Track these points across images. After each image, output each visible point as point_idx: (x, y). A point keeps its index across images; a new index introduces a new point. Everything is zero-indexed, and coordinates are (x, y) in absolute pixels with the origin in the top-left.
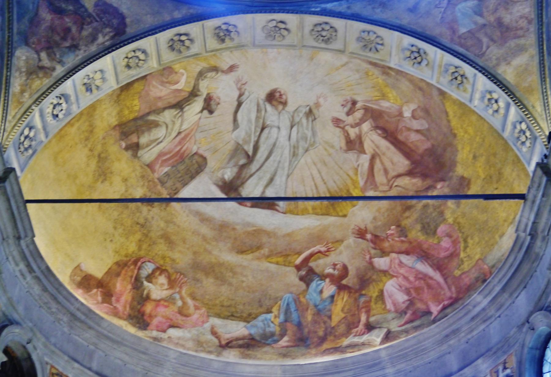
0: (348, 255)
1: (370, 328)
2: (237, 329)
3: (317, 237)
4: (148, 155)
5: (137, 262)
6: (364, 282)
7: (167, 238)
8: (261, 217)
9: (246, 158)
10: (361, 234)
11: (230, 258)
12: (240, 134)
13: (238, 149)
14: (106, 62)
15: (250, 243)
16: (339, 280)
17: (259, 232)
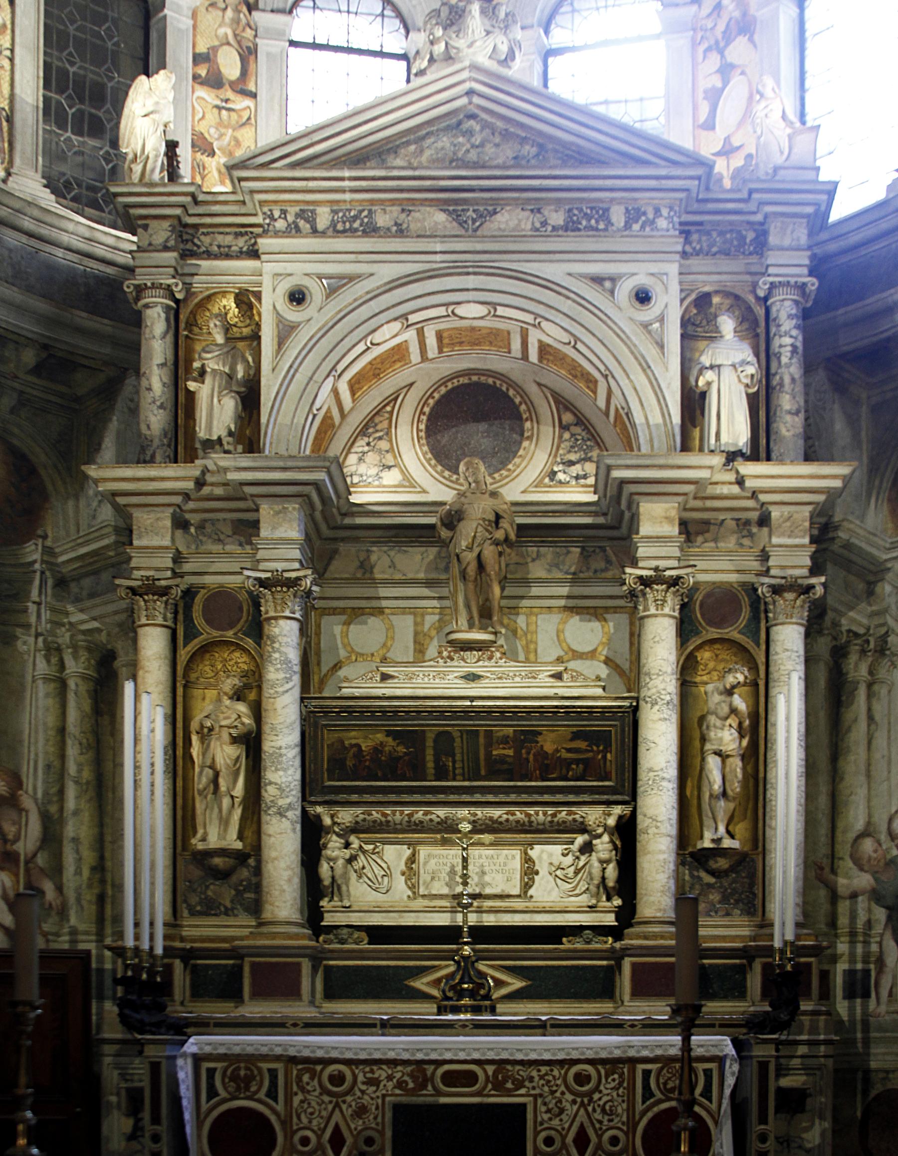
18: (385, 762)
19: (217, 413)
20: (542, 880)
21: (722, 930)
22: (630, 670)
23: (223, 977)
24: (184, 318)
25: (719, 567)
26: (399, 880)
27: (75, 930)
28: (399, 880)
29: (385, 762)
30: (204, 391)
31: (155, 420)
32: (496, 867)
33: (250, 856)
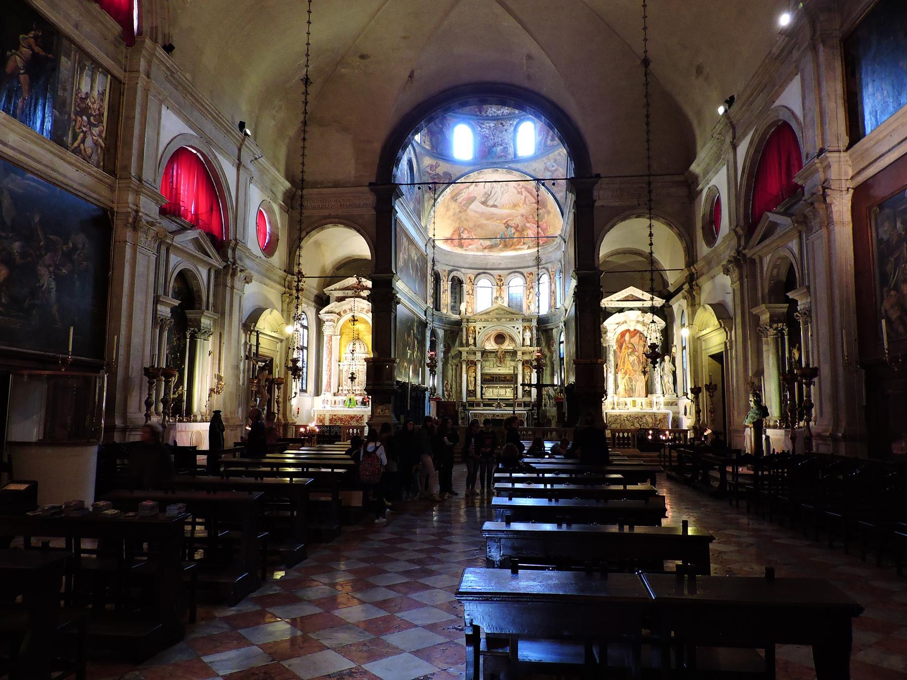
0: (518, 221)
1: (524, 244)
2: (488, 243)
3: (510, 216)
4: (459, 201)
5: (459, 229)
6: (523, 230)
7: (466, 220)
8: (494, 210)
9: (488, 195)
10: (522, 216)
11: (485, 222)
12: (486, 190)
13: (486, 193)
14: (448, 190)
15: (491, 217)
16: (516, 228)
17: (493, 214)
18: (490, 380)
19: (471, 341)
20: (508, 393)
21: (527, 399)
22: (515, 368)
23: (472, 404)
24: (467, 330)
25: (527, 358)
26: (492, 393)
27: (453, 399)
28: (492, 393)
29: (490, 380)
30: (470, 339)
31: (464, 342)
32: (502, 391)
33: (475, 391)
